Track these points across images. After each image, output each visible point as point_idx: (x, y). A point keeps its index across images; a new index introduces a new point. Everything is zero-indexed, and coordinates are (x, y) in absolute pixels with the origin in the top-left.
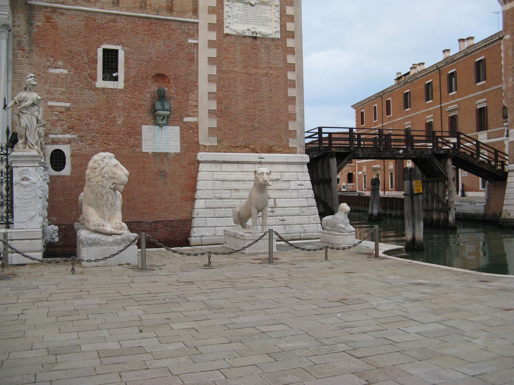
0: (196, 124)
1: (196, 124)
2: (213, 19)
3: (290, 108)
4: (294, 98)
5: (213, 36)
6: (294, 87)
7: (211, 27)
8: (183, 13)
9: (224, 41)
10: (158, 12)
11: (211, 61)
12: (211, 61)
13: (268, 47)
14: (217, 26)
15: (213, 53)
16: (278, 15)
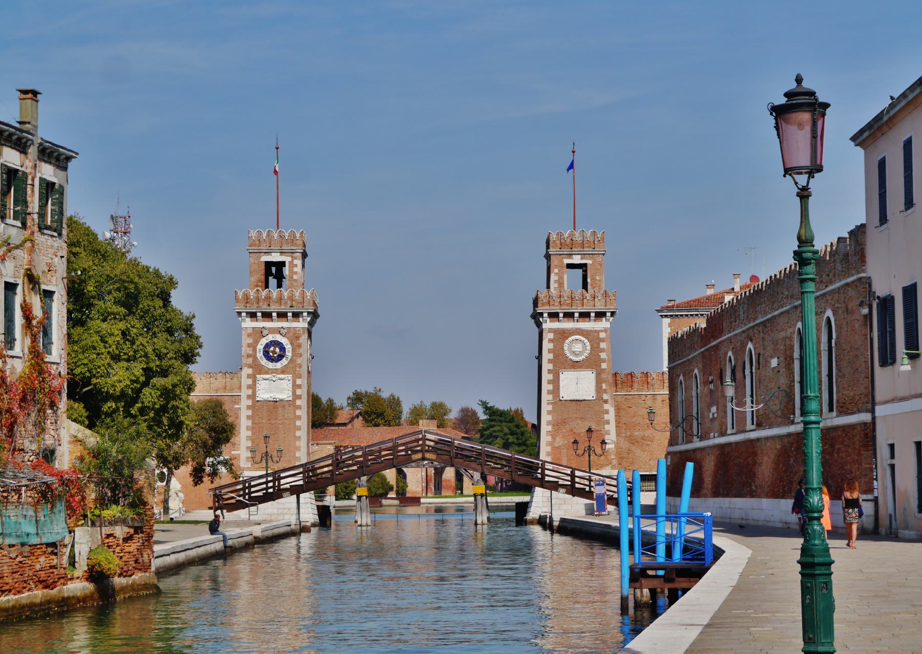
0: (239, 455)
1: (239, 455)
2: (250, 392)
3: (297, 443)
4: (300, 437)
5: (250, 402)
6: (300, 429)
7: (249, 397)
8: (232, 390)
9: (257, 406)
10: (217, 391)
11: (248, 417)
12: (248, 417)
13: (284, 407)
14: (253, 396)
15: (250, 413)
16: (291, 386)
